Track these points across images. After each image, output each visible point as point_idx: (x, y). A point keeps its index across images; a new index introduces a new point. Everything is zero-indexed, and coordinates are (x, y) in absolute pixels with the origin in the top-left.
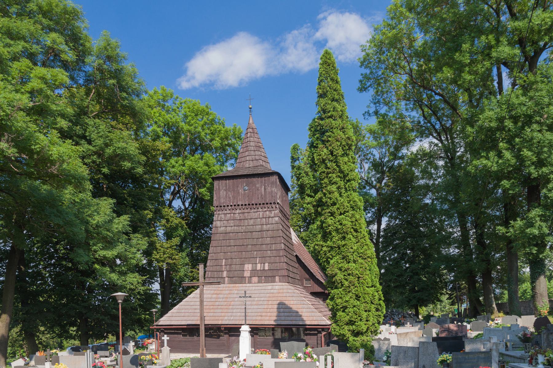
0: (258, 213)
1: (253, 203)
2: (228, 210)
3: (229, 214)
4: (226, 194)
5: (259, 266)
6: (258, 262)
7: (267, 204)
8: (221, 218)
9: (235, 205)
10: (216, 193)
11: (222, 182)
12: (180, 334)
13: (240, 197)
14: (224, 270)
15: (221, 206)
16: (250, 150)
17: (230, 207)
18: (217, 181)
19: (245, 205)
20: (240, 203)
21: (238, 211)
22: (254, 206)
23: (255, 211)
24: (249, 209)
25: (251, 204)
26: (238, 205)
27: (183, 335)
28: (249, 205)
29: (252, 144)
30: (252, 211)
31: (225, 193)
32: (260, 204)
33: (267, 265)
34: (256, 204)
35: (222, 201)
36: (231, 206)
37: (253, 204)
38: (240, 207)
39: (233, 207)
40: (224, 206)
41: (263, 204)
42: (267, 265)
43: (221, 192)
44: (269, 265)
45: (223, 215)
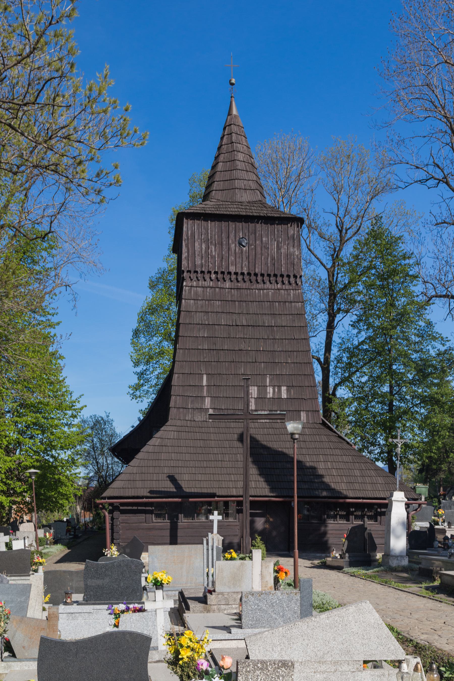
0: (265, 291)
1: (257, 271)
2: (208, 279)
3: (212, 287)
4: (208, 248)
5: (270, 390)
6: (268, 384)
7: (282, 276)
8: (196, 293)
9: (223, 273)
10: (187, 246)
11: (198, 225)
12: (151, 512)
13: (233, 258)
14: (205, 394)
15: (196, 272)
16: (239, 167)
17: (213, 276)
18: (190, 222)
19: (243, 274)
20: (232, 269)
21: (228, 284)
22: (260, 278)
23: (260, 286)
24: (248, 283)
25: (252, 273)
26: (229, 273)
27: (158, 516)
28: (249, 274)
29: (240, 156)
30: (254, 287)
31: (204, 246)
32: (269, 275)
33: (284, 389)
34: (262, 275)
35: (198, 261)
36: (216, 273)
37: (256, 275)
38: (233, 277)
39: (220, 276)
40: (202, 272)
41: (275, 275)
42: (284, 389)
43: (197, 244)
44: (288, 391)
45: (199, 289)
